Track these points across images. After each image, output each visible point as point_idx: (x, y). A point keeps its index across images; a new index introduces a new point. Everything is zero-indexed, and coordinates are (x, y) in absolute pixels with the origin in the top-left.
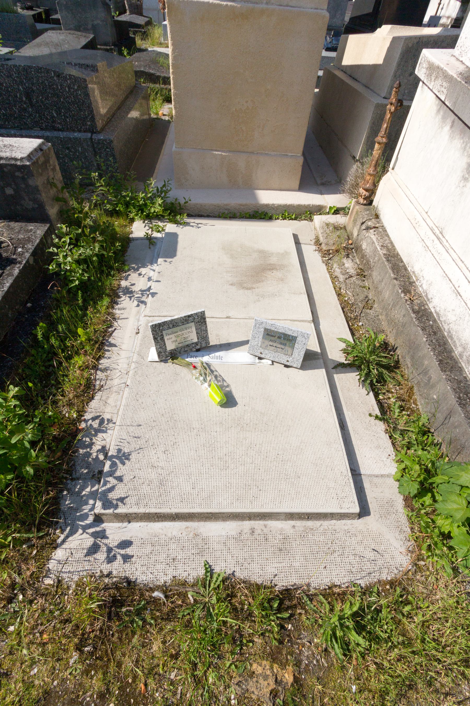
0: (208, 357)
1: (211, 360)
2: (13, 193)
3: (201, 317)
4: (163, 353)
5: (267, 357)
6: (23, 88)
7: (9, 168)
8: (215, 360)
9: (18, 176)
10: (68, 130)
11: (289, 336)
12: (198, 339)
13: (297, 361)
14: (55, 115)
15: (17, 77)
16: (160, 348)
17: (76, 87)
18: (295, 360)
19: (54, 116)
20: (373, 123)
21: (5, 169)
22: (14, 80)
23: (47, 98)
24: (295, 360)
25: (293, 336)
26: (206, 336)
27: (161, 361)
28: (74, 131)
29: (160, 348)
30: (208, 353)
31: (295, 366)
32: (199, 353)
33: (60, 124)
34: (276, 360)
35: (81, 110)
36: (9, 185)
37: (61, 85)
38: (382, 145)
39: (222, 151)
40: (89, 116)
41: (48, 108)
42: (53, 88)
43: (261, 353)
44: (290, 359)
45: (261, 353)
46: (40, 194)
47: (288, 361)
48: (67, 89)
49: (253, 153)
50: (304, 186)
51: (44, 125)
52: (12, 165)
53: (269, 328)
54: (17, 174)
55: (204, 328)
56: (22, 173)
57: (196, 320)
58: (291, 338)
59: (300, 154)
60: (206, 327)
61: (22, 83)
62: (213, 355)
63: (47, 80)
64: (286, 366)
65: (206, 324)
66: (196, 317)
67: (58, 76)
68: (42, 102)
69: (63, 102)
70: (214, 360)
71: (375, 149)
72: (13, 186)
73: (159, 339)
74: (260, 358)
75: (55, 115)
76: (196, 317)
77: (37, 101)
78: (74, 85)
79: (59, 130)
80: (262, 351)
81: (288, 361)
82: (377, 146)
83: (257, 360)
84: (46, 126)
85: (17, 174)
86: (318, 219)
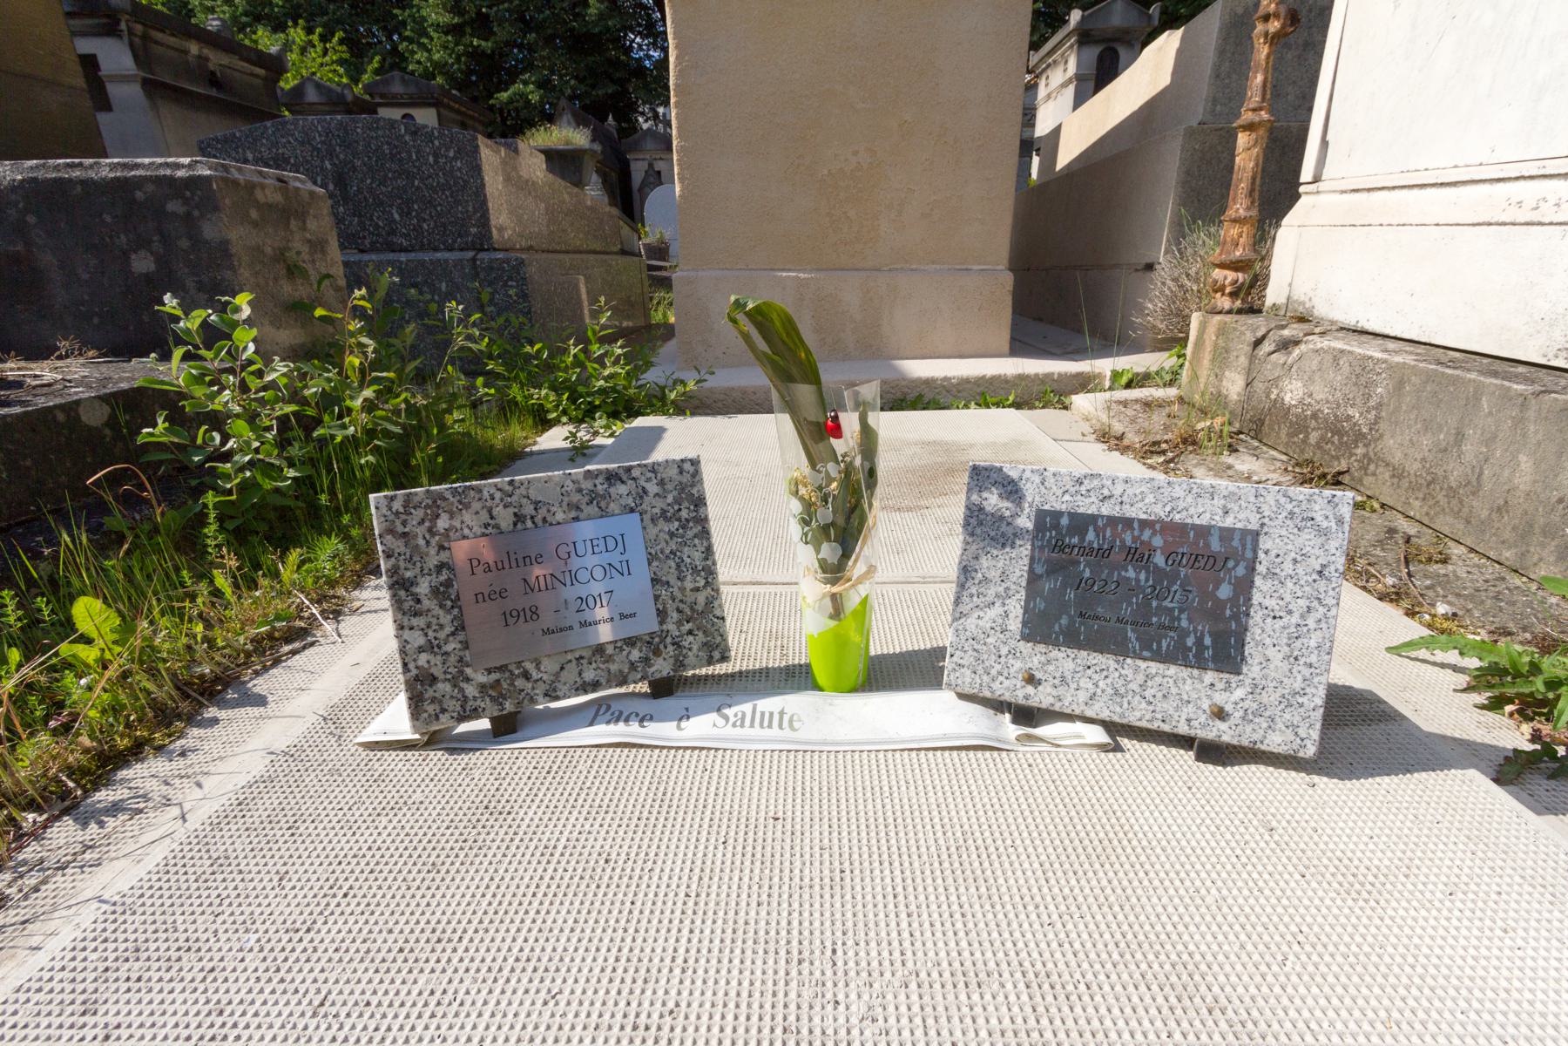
0: (713, 717)
1: (729, 731)
2: (152, 267)
3: (682, 488)
4: (444, 687)
5: (1072, 700)
6: (333, 164)
7: (150, 188)
8: (757, 731)
9: (173, 213)
10: (422, 248)
11: (1203, 531)
12: (662, 615)
13: (1287, 702)
14: (397, 216)
15: (323, 143)
16: (430, 647)
17: (451, 154)
18: (1270, 697)
19: (394, 221)
20: (1188, 173)
21: (139, 195)
22: (315, 149)
23: (383, 183)
24: (1270, 697)
25: (1227, 534)
26: (710, 602)
27: (432, 741)
28: (436, 250)
29: (430, 647)
30: (716, 700)
31: (1276, 742)
32: (666, 703)
33: (405, 236)
34: (1137, 715)
35: (457, 202)
36: (142, 243)
37: (418, 152)
38: (1261, 132)
39: (799, 271)
40: (475, 212)
41: (382, 203)
42: (401, 160)
43: (1031, 680)
44: (1233, 695)
45: (1031, 680)
46: (231, 267)
47: (1220, 714)
48: (431, 159)
49: (878, 270)
50: (1020, 346)
51: (367, 242)
52: (159, 180)
53: (1061, 504)
54: (174, 206)
55: (695, 555)
56: (186, 201)
57: (654, 505)
58: (1215, 545)
59: (1003, 264)
60: (709, 552)
61: (331, 154)
62: (747, 708)
63: (388, 143)
64: (1213, 753)
65: (705, 534)
66: (652, 488)
67: (415, 133)
68: (371, 190)
69: (418, 188)
70: (747, 731)
71: (1239, 149)
72: (156, 246)
73: (423, 588)
74: (1026, 716)
75: (397, 216)
76: (652, 488)
77: (360, 191)
78: (447, 150)
79: (406, 250)
80: (1035, 662)
81: (1220, 714)
82: (1243, 139)
83: (1009, 729)
84: (372, 243)
85: (174, 206)
86: (1080, 401)
